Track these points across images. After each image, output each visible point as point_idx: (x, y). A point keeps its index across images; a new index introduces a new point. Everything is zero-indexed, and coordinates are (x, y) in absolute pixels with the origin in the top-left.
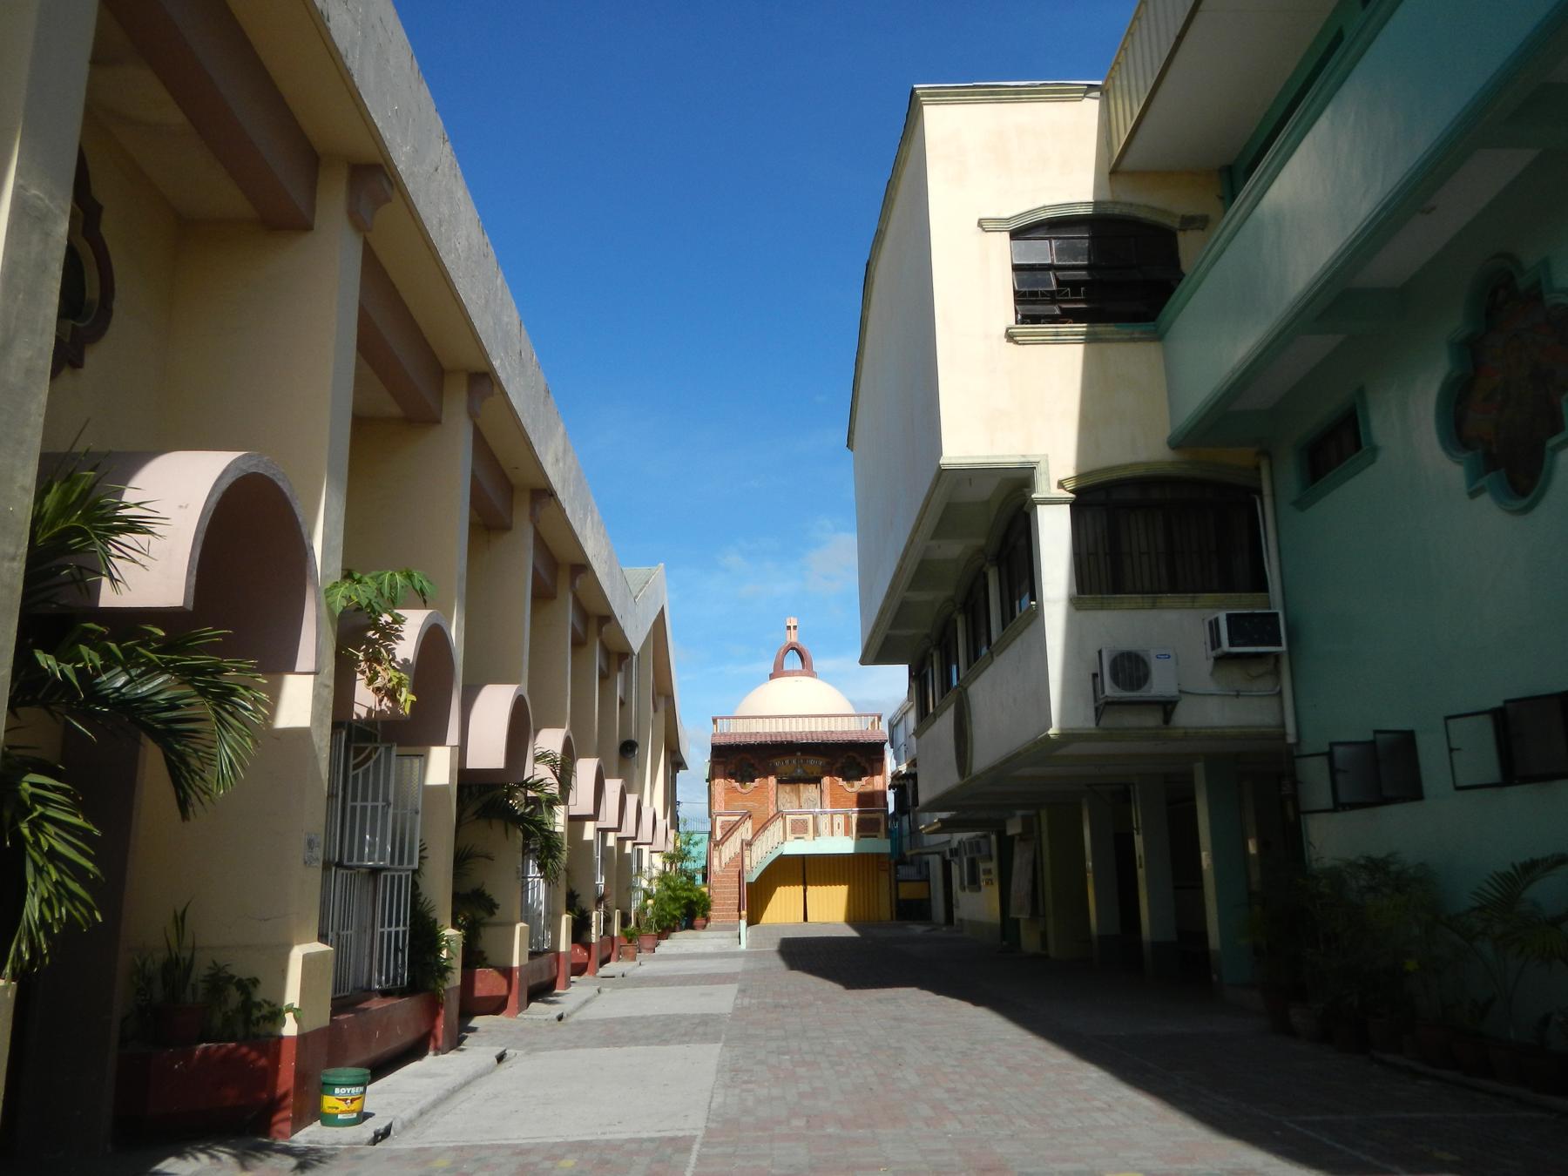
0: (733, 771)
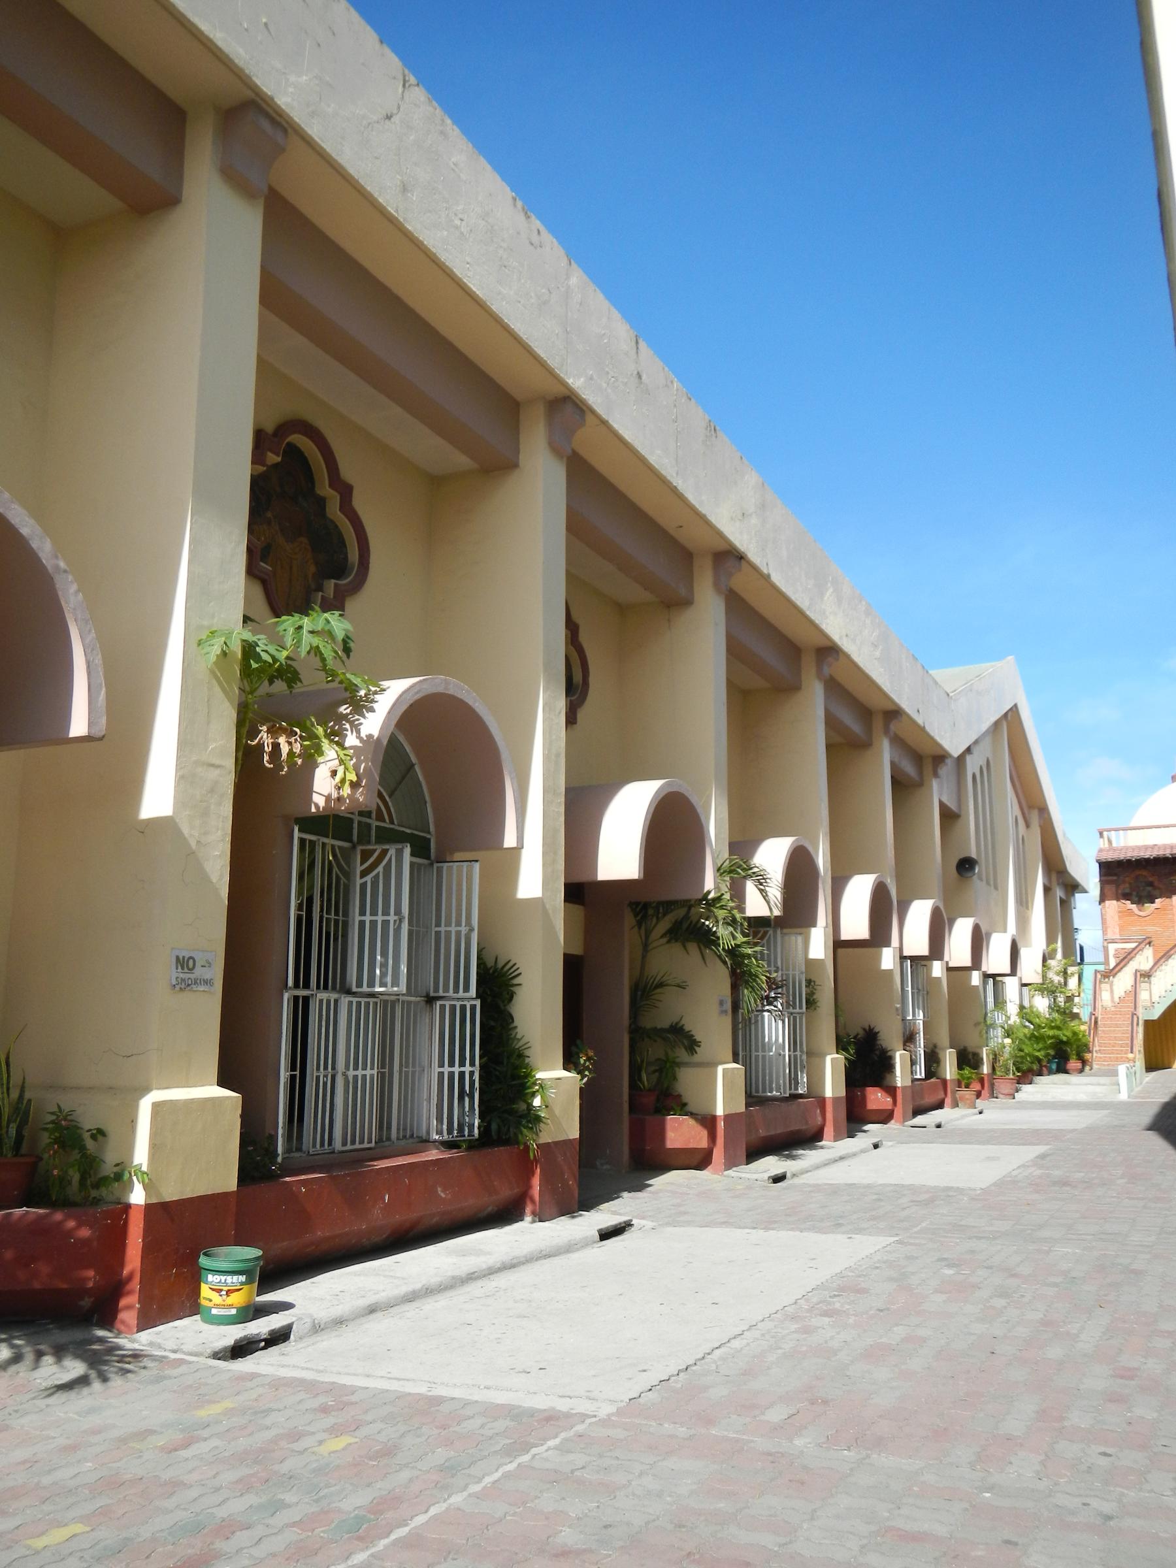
0: (1127, 891)
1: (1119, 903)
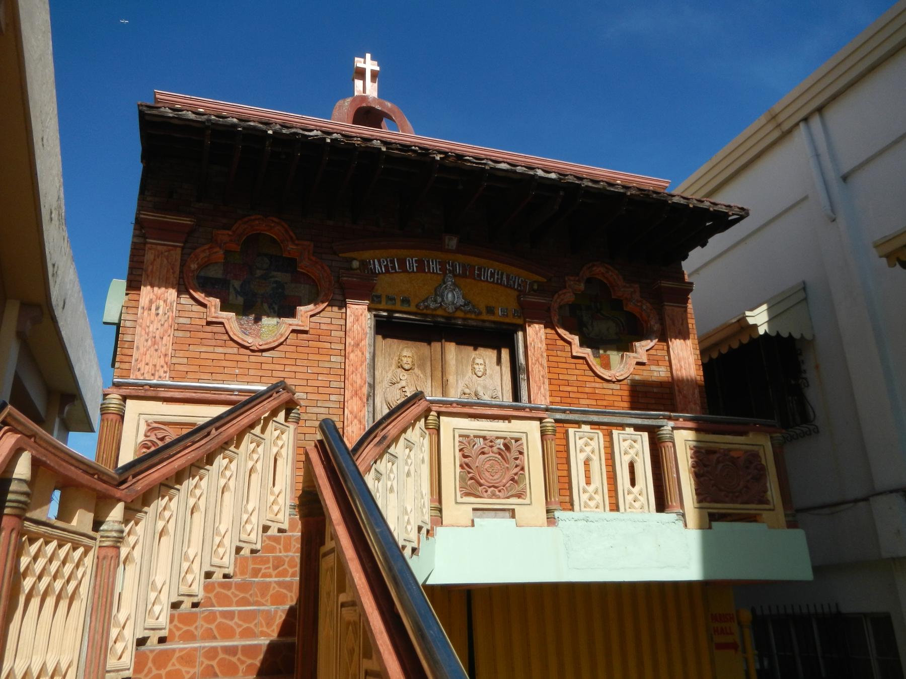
0: (215, 272)
1: (185, 300)
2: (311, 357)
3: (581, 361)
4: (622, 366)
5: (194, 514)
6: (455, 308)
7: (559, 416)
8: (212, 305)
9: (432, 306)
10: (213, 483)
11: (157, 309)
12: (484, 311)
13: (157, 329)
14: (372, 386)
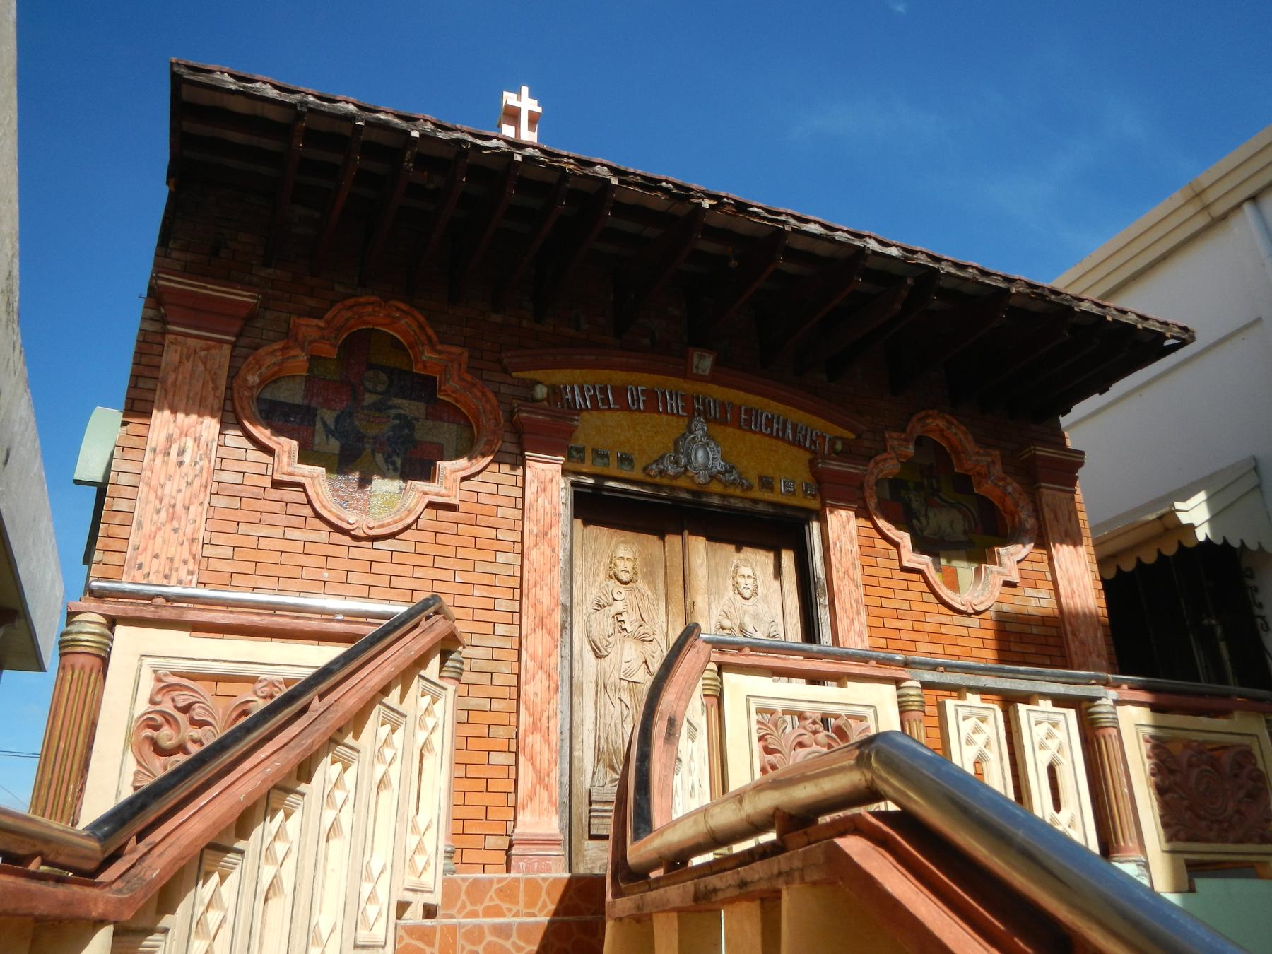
0: (291, 393)
1: (234, 439)
2: (461, 553)
3: (915, 577)
4: (979, 588)
5: (270, 902)
6: (710, 476)
7: (929, 676)
8: (283, 451)
9: (672, 470)
10: (310, 826)
11: (181, 452)
12: (756, 484)
13: (180, 491)
14: (569, 610)
